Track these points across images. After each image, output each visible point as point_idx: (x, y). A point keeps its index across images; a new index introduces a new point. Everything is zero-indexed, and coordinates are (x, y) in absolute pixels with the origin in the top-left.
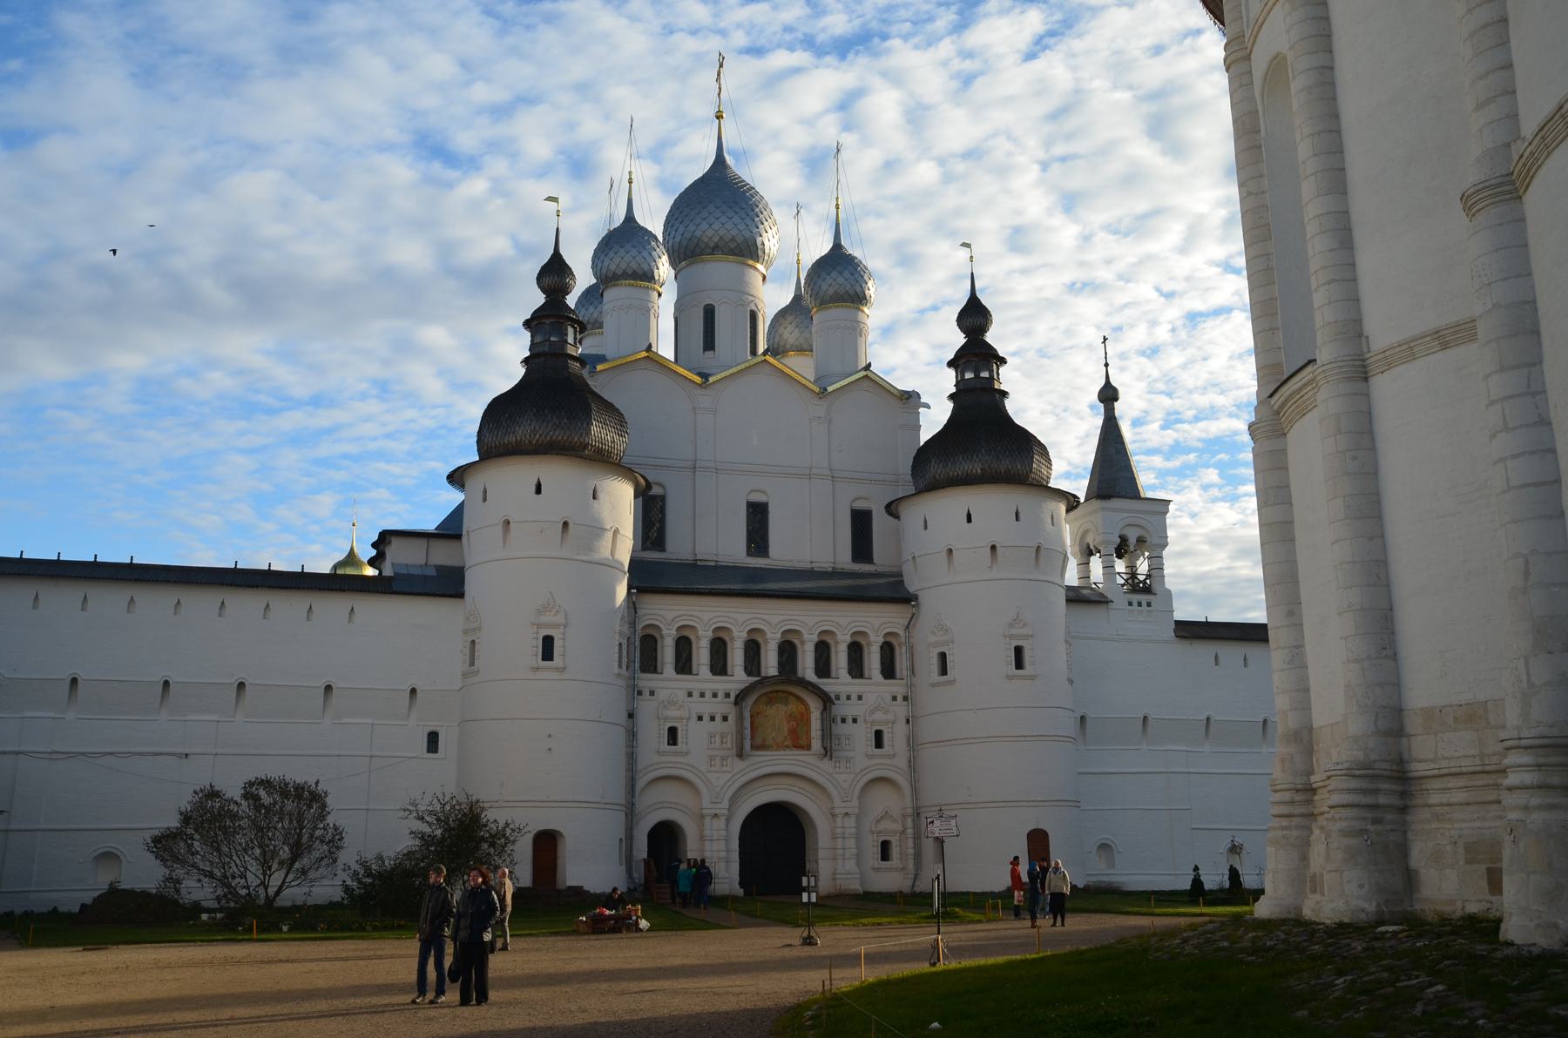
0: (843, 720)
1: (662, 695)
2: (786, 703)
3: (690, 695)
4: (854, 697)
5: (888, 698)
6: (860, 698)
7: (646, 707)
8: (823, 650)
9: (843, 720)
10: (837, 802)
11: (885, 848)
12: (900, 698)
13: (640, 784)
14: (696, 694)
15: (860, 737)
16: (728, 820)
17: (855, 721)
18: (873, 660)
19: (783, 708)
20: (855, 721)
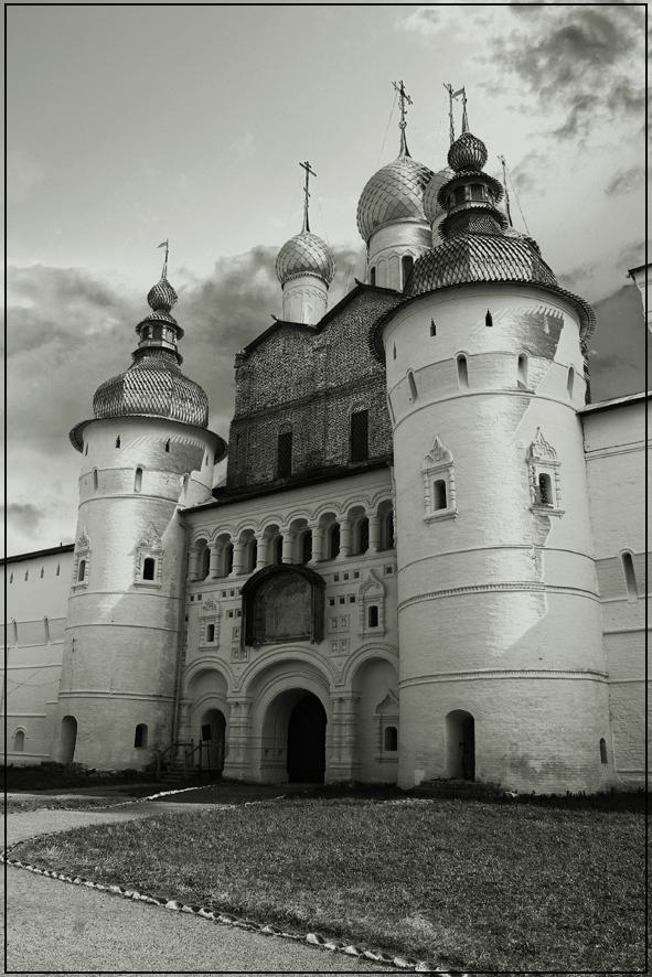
0: (342, 601)
1: (205, 598)
3: (224, 595)
4: (351, 575)
7: (196, 610)
9: (342, 601)
10: (332, 689)
13: (189, 675)
15: (355, 615)
16: (251, 706)
17: (353, 600)
20: (353, 600)
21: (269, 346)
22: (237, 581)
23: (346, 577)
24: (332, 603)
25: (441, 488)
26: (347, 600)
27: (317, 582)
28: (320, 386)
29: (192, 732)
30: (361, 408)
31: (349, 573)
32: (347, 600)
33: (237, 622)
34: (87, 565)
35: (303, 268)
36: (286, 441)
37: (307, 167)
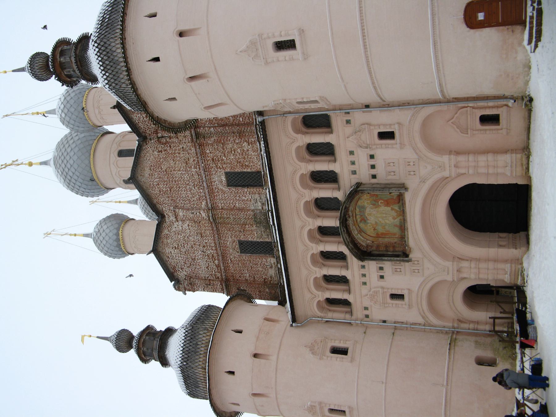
0: (373, 167)
1: (367, 303)
2: (363, 208)
3: (365, 284)
5: (349, 130)
6: (352, 153)
7: (377, 314)
8: (319, 178)
9: (373, 167)
10: (446, 174)
11: (486, 120)
12: (348, 117)
14: (364, 280)
15: (386, 152)
17: (372, 157)
18: (318, 138)
19: (368, 211)
20: (372, 157)
21: (172, 262)
22: (353, 269)
23: (353, 163)
24: (374, 177)
25: (281, 46)
26: (372, 162)
27: (357, 190)
28: (204, 215)
29: (482, 316)
30: (224, 178)
31: (352, 163)
32: (372, 162)
33: (388, 265)
34: (332, 407)
35: (118, 240)
36: (247, 247)
37: (47, 234)
